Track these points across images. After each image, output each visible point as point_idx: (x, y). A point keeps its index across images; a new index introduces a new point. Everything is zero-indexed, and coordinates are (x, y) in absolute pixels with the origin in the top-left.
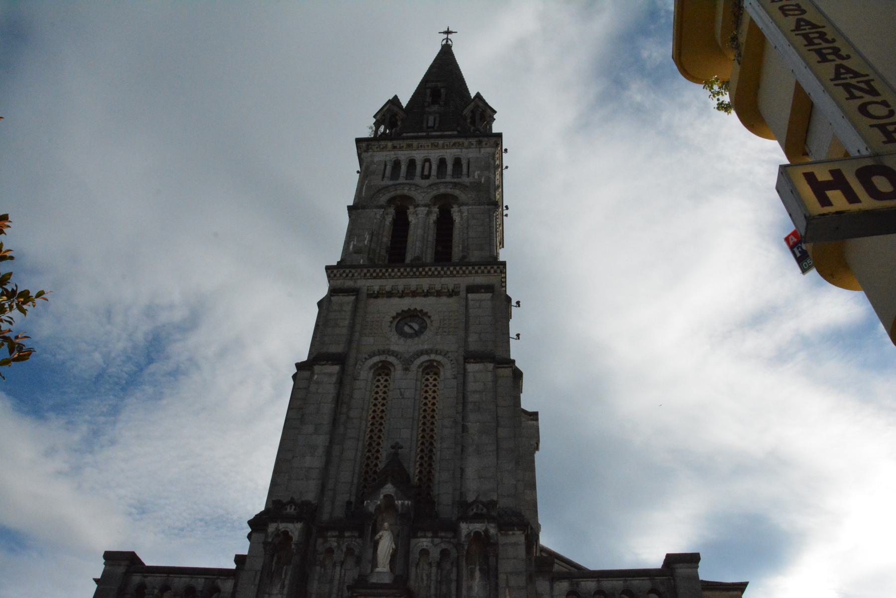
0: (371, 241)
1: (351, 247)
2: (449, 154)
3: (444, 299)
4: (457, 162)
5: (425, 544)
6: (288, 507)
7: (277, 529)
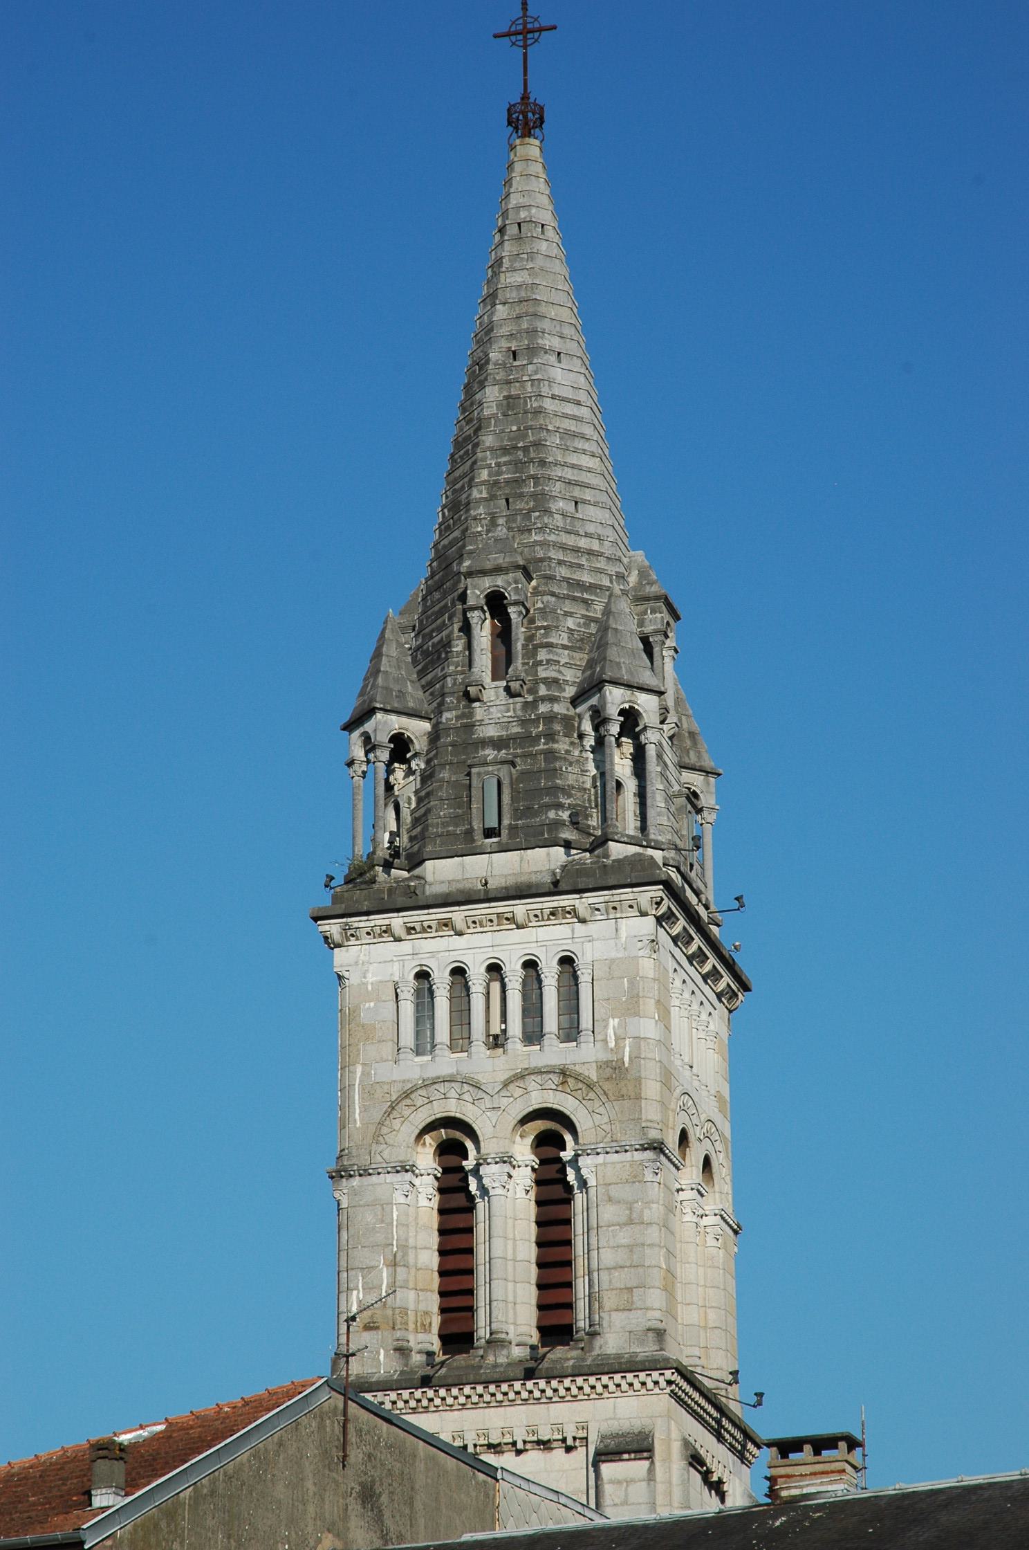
2: (546, 941)
4: (567, 961)
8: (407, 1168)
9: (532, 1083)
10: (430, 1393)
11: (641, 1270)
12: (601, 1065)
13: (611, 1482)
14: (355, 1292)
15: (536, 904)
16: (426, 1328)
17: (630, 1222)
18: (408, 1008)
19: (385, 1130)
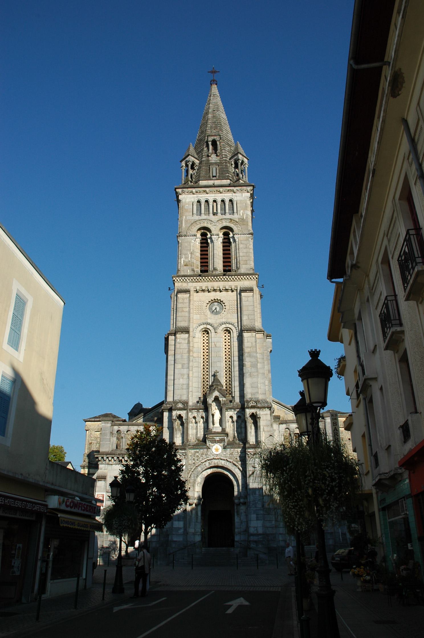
0: (191, 258)
1: (182, 262)
2: (227, 196)
4: (231, 201)
8: (195, 235)
9: (223, 221)
10: (201, 278)
15: (225, 189)
16: (198, 268)
17: (246, 248)
18: (195, 207)
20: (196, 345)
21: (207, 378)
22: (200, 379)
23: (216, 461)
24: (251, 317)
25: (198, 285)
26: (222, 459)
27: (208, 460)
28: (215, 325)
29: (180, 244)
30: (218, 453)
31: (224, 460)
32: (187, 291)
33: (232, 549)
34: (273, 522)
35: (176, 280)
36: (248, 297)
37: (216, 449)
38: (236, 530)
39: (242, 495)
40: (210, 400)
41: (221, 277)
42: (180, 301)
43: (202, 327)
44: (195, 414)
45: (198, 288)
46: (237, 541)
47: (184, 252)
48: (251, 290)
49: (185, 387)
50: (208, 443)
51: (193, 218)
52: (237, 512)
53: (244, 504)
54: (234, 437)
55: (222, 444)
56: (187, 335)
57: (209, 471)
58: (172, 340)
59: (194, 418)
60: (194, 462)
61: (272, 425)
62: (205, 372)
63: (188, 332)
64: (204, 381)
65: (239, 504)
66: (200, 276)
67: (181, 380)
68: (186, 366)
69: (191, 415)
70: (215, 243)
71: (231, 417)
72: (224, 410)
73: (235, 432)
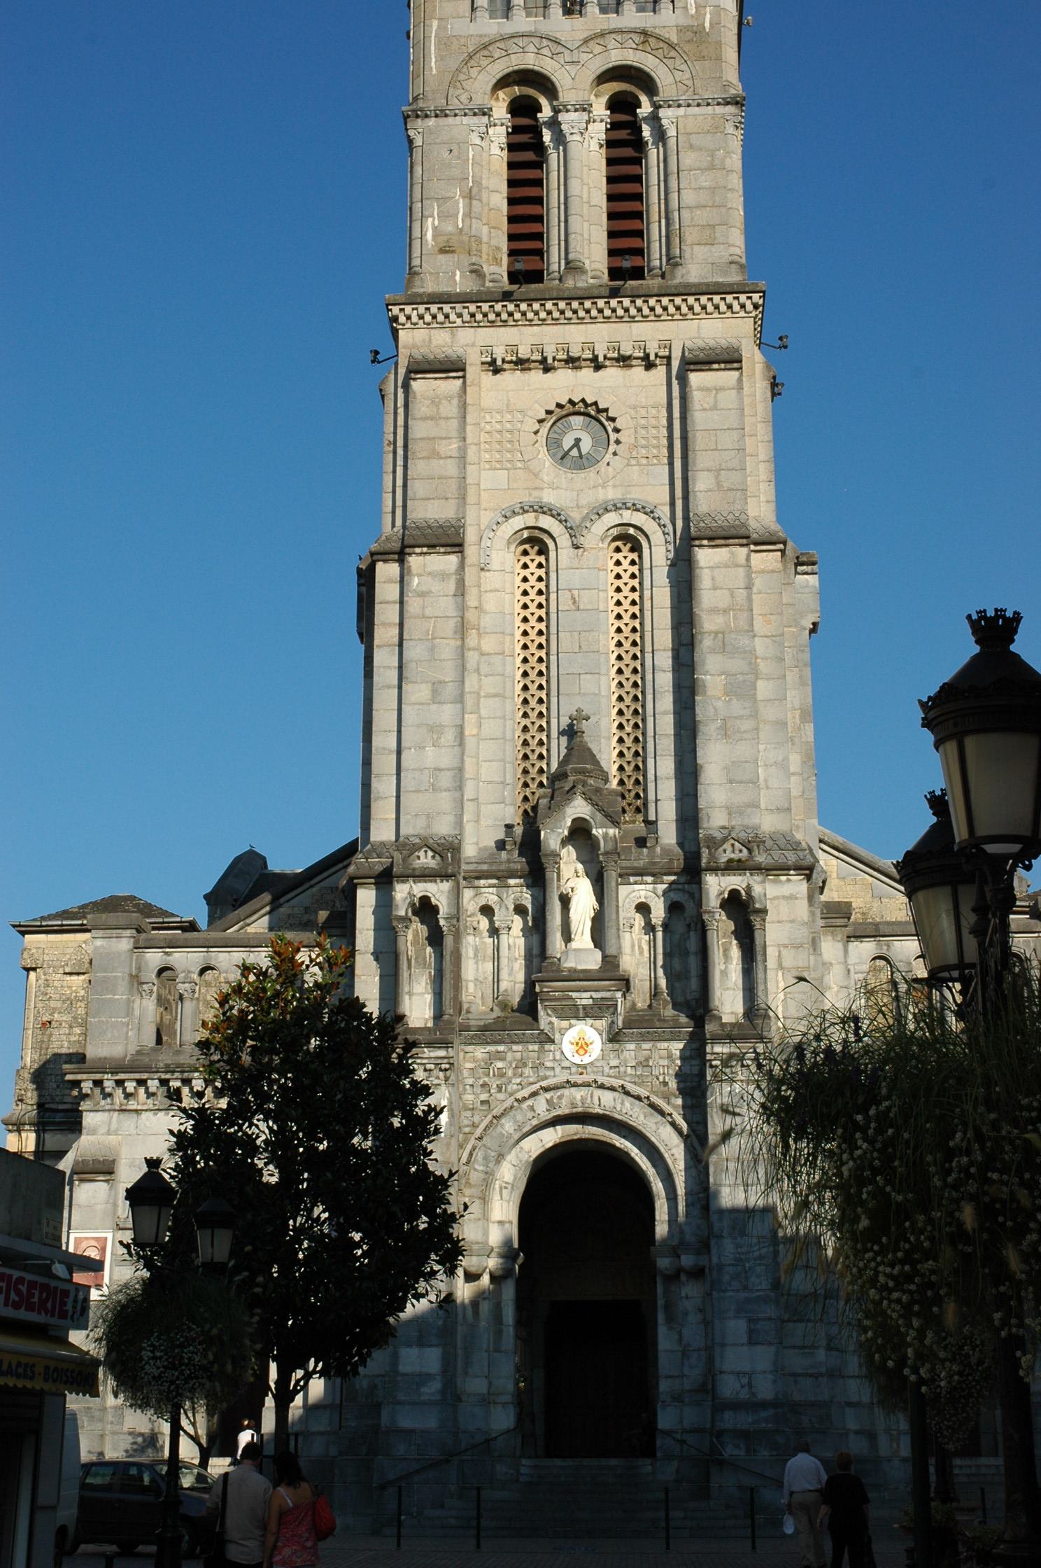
0: (468, 215)
3: (638, 372)
5: (643, 893)
6: (422, 854)
7: (411, 895)
8: (485, 112)
9: (611, 42)
10: (511, 307)
11: (723, 210)
12: (681, 30)
13: (700, 389)
14: (430, 220)
16: (497, 262)
17: (712, 167)
19: (462, 77)
20: (490, 602)
21: (541, 743)
22: (509, 747)
23: (578, 1094)
24: (730, 479)
25: (501, 340)
26: (602, 1087)
27: (546, 1089)
28: (576, 516)
29: (417, 155)
30: (586, 1060)
31: (612, 1089)
32: (452, 367)
33: (646, 1466)
34: (821, 1354)
35: (402, 319)
36: (719, 389)
37: (580, 1041)
38: (664, 1386)
39: (689, 1238)
40: (552, 837)
41: (601, 303)
42: (420, 408)
43: (518, 522)
44: (490, 895)
45: (499, 353)
46: (668, 1433)
47: (436, 187)
48: (731, 359)
49: (446, 780)
50: (546, 1019)
51: (473, 29)
52: (668, 1307)
53: (698, 1273)
54: (655, 993)
55: (602, 1024)
56: (453, 559)
57: (551, 1137)
58: (390, 581)
59: (487, 910)
60: (484, 1097)
61: (815, 944)
62: (533, 715)
63: (456, 546)
64: (526, 757)
65: (674, 1277)
66: (507, 296)
67: (430, 750)
68: (450, 690)
69: (470, 900)
70: (574, 149)
71: (643, 908)
72: (611, 876)
73: (660, 972)
